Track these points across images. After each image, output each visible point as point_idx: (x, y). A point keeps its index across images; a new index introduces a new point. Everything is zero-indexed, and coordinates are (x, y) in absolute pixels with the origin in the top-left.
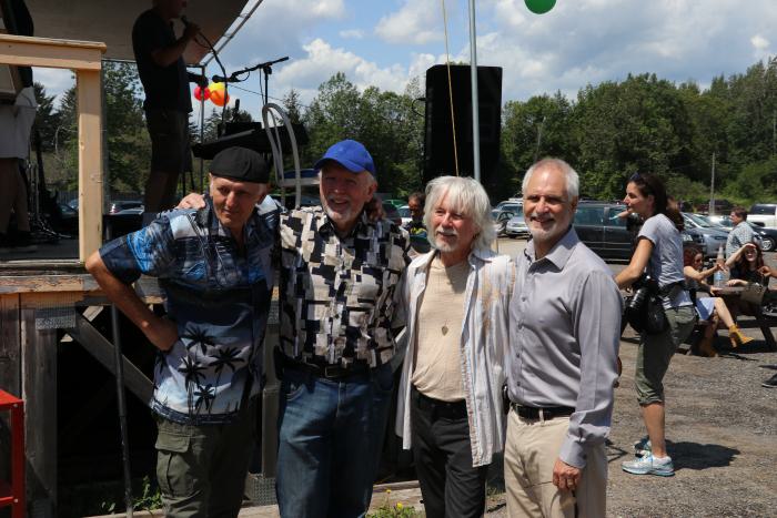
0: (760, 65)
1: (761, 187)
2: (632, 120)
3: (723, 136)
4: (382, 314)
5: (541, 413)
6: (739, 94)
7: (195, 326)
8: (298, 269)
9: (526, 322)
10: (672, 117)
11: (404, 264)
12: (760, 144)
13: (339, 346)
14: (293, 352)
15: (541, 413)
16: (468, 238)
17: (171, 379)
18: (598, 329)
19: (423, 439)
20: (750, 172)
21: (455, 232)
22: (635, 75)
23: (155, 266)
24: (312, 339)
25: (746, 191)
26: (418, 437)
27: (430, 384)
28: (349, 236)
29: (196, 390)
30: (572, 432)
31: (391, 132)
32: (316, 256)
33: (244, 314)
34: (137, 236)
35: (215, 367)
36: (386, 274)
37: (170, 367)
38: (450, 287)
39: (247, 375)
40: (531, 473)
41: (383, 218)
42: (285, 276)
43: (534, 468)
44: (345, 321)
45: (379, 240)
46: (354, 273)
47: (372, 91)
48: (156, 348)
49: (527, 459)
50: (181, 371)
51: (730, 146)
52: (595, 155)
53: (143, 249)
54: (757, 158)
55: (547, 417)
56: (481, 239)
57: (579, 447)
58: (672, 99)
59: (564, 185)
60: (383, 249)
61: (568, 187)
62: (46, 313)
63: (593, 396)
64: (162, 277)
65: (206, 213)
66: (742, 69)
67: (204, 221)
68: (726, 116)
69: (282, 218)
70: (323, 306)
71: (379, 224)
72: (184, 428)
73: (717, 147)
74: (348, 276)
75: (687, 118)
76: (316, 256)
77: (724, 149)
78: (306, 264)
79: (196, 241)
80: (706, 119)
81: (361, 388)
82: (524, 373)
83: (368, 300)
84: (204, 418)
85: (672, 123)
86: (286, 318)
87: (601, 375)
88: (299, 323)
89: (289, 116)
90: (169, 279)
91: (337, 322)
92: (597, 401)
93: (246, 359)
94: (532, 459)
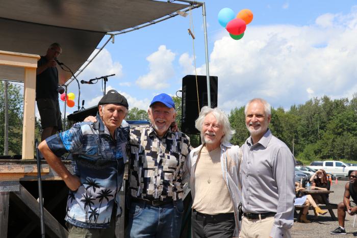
0: (311, 101)
1: (314, 155)
3: (296, 132)
4: (178, 176)
5: (260, 216)
6: (302, 113)
7: (90, 178)
8: (139, 154)
9: (250, 173)
10: (273, 122)
11: (188, 152)
12: (313, 136)
13: (159, 190)
14: (135, 194)
15: (260, 216)
16: (220, 137)
17: (77, 205)
18: (285, 174)
19: (198, 235)
20: (309, 148)
21: (214, 134)
23: (73, 148)
24: (146, 187)
25: (308, 157)
26: (196, 235)
27: (203, 207)
28: (164, 138)
29: (90, 210)
30: (276, 223)
32: (148, 147)
33: (113, 172)
34: (64, 134)
35: (99, 199)
36: (180, 156)
37: (77, 199)
38: (211, 161)
39: (114, 205)
41: (178, 130)
42: (132, 157)
44: (162, 177)
45: (177, 140)
46: (166, 155)
48: (69, 189)
50: (82, 201)
51: (299, 136)
52: (239, 140)
53: (67, 139)
54: (312, 142)
55: (263, 218)
56: (225, 138)
57: (279, 230)
59: (264, 109)
60: (178, 144)
61: (266, 110)
62: (5, 184)
63: (285, 205)
64: (75, 153)
65: (98, 123)
66: (304, 102)
67: (97, 127)
68: (297, 123)
69: (131, 130)
70: (151, 171)
71: (176, 133)
72: (83, 230)
74: (163, 156)
75: (280, 123)
76: (148, 147)
77: (296, 137)
78: (144, 151)
79: (92, 136)
80: (288, 124)
81: (169, 211)
82: (251, 197)
83: (173, 168)
84: (93, 225)
85: (273, 125)
86: (133, 178)
87: (289, 195)
88: (141, 179)
90: (77, 155)
91: (159, 178)
92: (287, 208)
93: (114, 195)
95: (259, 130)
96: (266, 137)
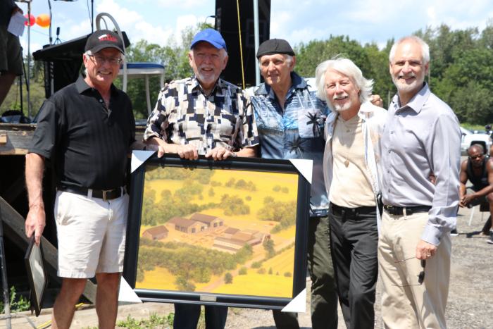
5: (404, 211)
9: (393, 148)
15: (404, 211)
22: (335, 35)
30: (431, 221)
40: (398, 252)
43: (399, 249)
49: (395, 241)
55: (409, 213)
58: (360, 53)
59: (421, 53)
61: (424, 55)
73: (391, 89)
75: (370, 67)
94: (398, 243)
95: (414, 84)
96: (422, 94)
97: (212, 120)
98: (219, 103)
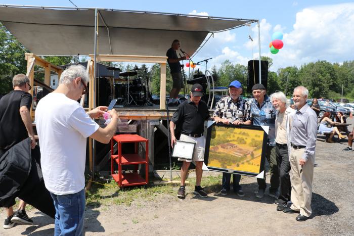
2: (317, 74)
31: (244, 77)
47: (237, 65)
55: (299, 148)
75: (335, 74)
77: (347, 83)
89: (213, 72)
97: (236, 111)
98: (238, 106)
